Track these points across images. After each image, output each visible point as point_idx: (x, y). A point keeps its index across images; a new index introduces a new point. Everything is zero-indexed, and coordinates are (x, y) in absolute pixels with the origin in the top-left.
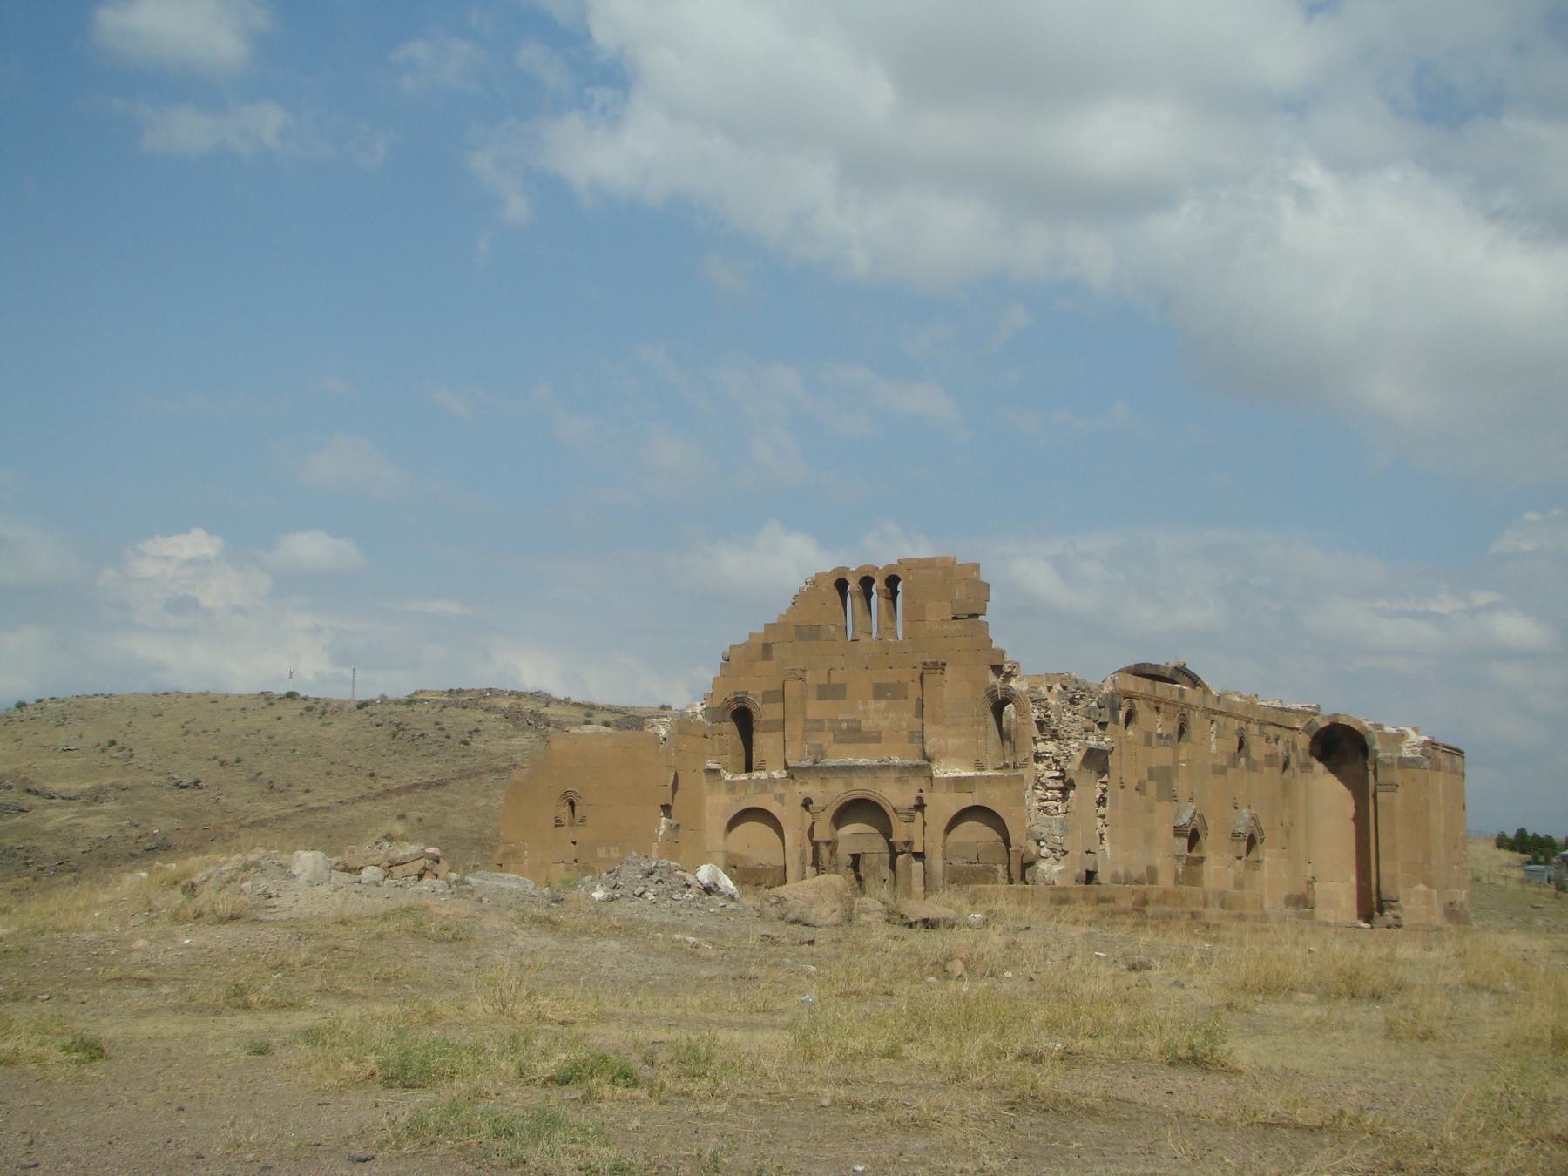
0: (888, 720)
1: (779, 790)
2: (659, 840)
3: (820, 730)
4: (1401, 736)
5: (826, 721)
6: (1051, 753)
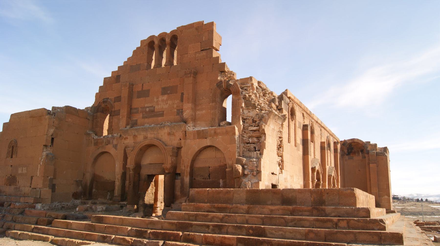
0: (168, 105)
1: (115, 142)
2: (41, 164)
3: (137, 112)
4: (376, 145)
5: (140, 108)
6: (252, 117)
